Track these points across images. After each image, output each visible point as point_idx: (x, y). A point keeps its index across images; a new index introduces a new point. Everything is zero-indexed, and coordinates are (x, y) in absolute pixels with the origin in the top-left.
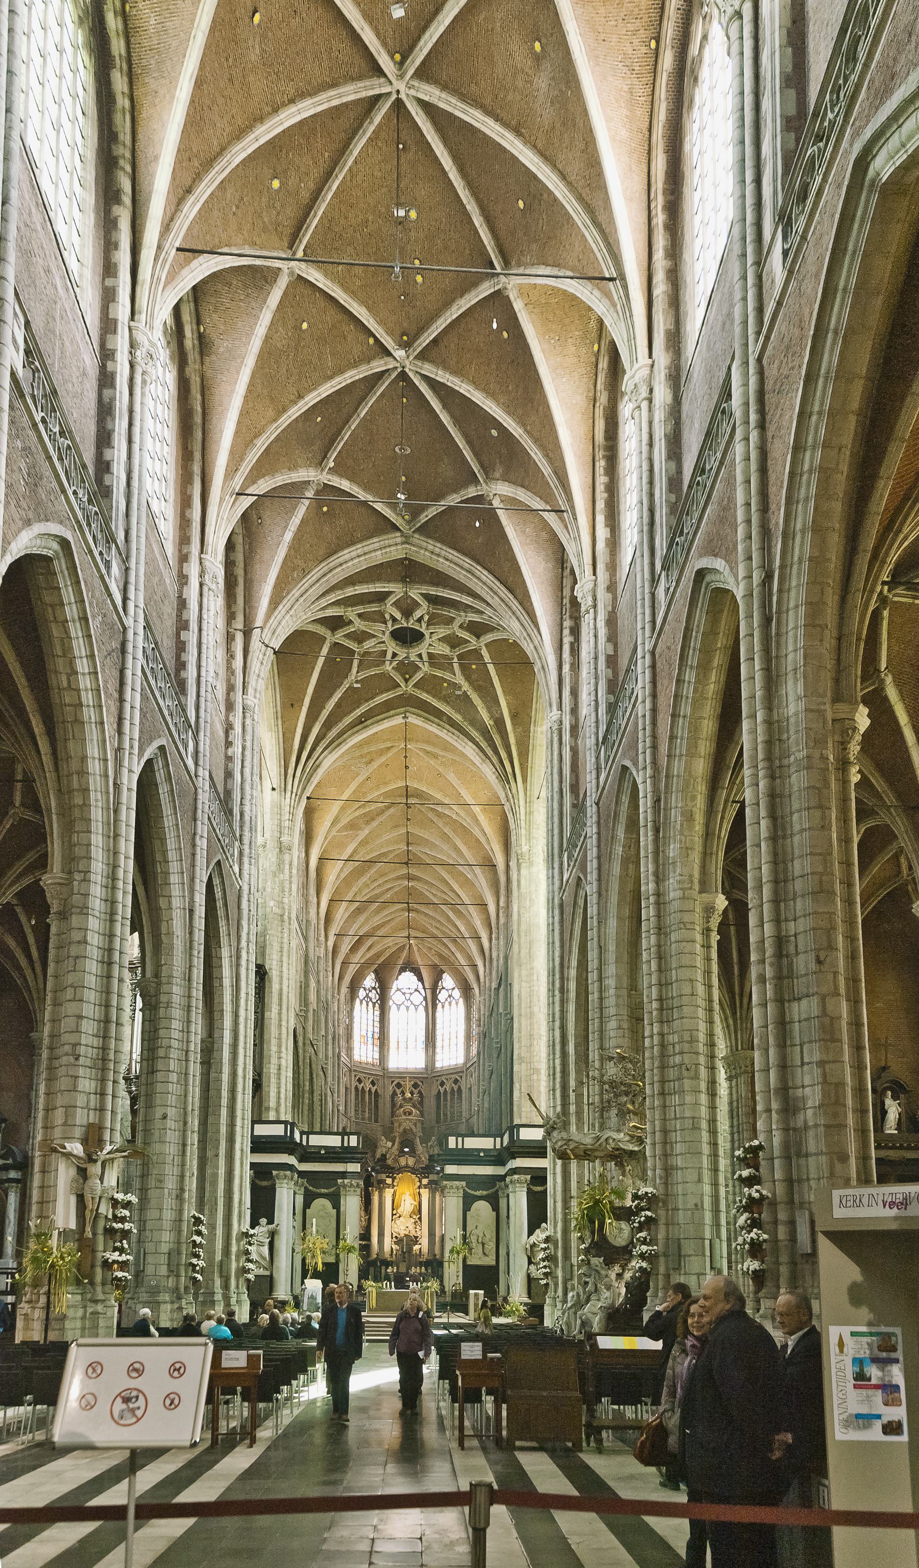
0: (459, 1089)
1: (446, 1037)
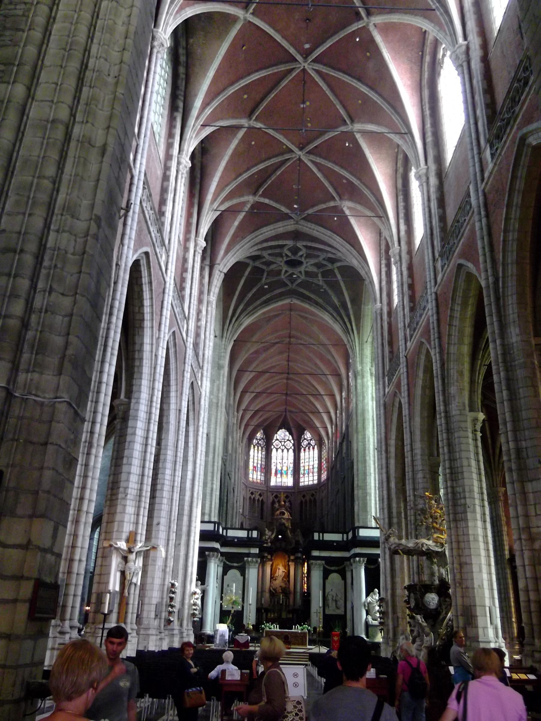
0: (315, 499)
1: (307, 468)
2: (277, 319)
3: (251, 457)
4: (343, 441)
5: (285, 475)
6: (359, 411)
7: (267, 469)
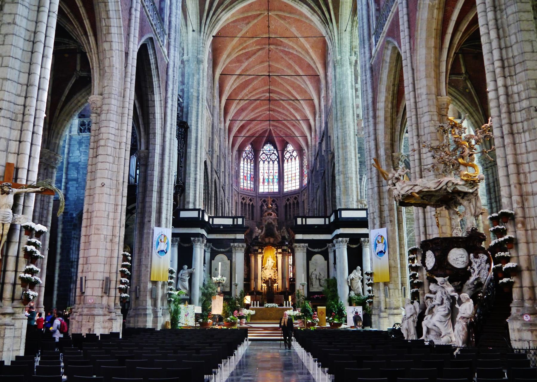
0: (298, 203)
1: (290, 176)
2: (256, 21)
3: (242, 168)
4: (322, 140)
5: (271, 184)
6: (338, 100)
7: (255, 178)
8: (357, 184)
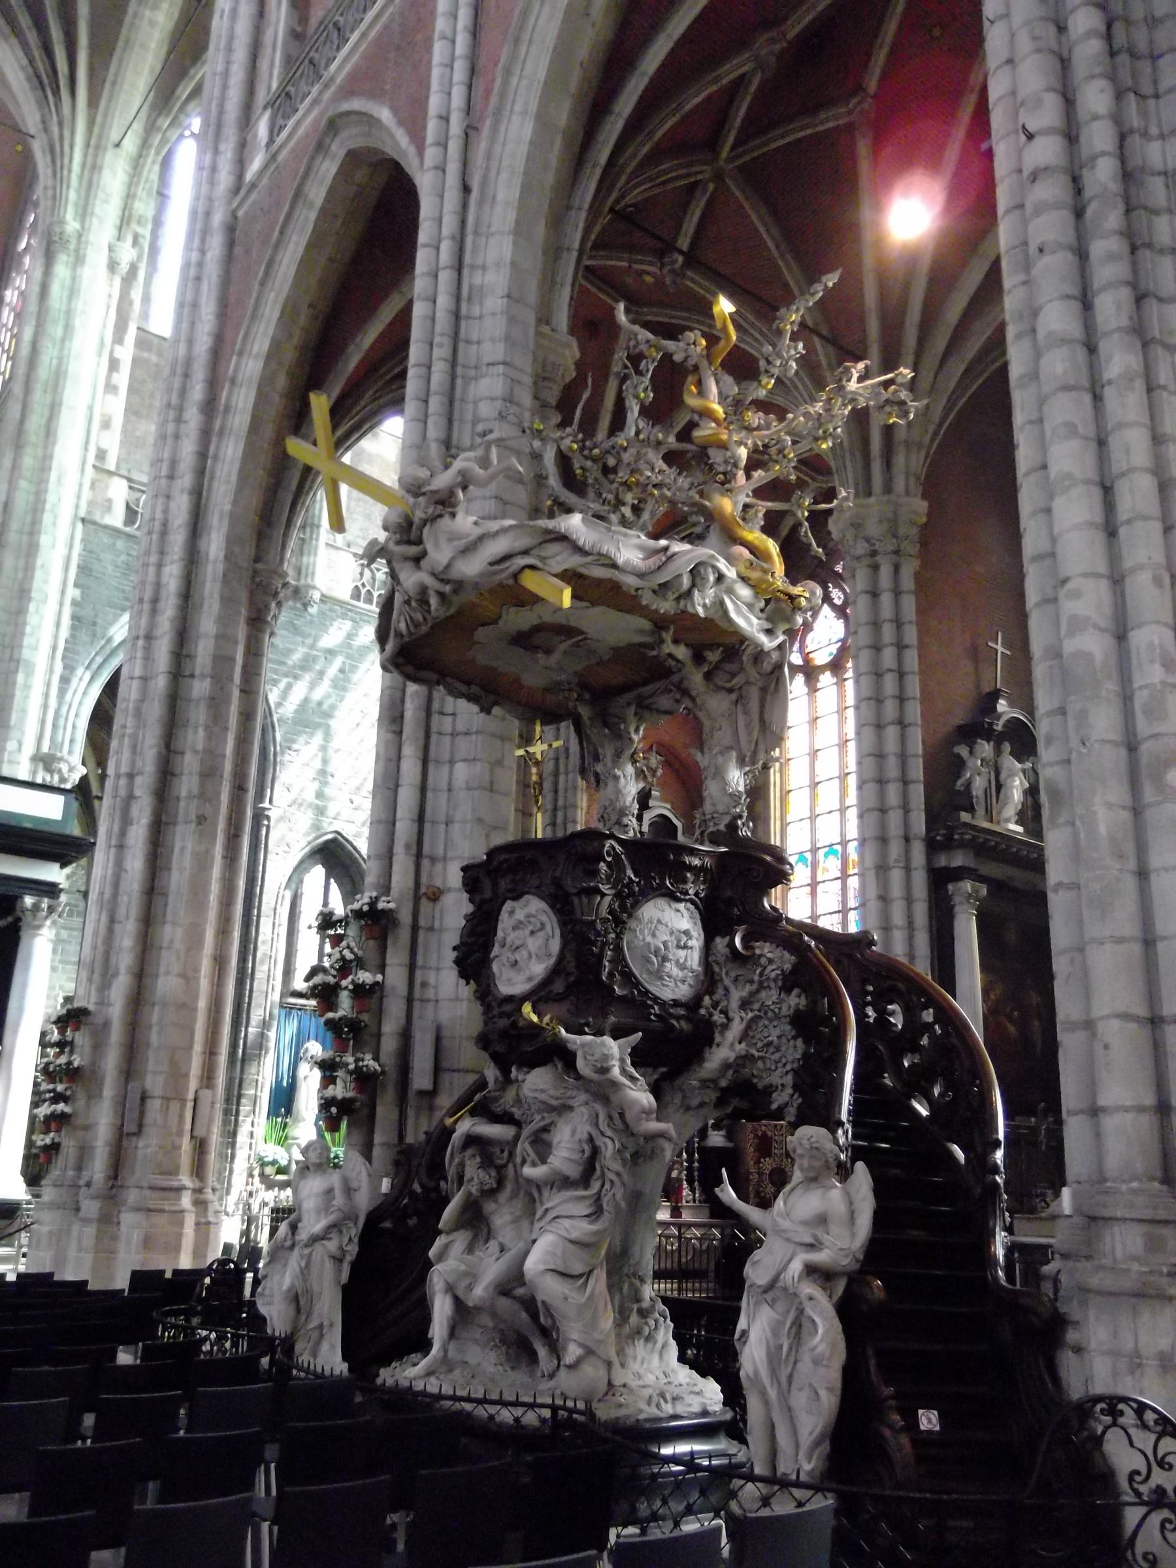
8: (47, 695)
